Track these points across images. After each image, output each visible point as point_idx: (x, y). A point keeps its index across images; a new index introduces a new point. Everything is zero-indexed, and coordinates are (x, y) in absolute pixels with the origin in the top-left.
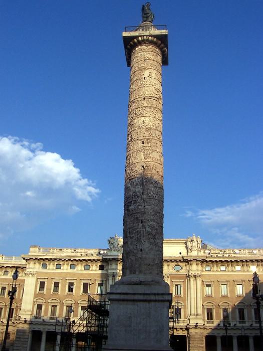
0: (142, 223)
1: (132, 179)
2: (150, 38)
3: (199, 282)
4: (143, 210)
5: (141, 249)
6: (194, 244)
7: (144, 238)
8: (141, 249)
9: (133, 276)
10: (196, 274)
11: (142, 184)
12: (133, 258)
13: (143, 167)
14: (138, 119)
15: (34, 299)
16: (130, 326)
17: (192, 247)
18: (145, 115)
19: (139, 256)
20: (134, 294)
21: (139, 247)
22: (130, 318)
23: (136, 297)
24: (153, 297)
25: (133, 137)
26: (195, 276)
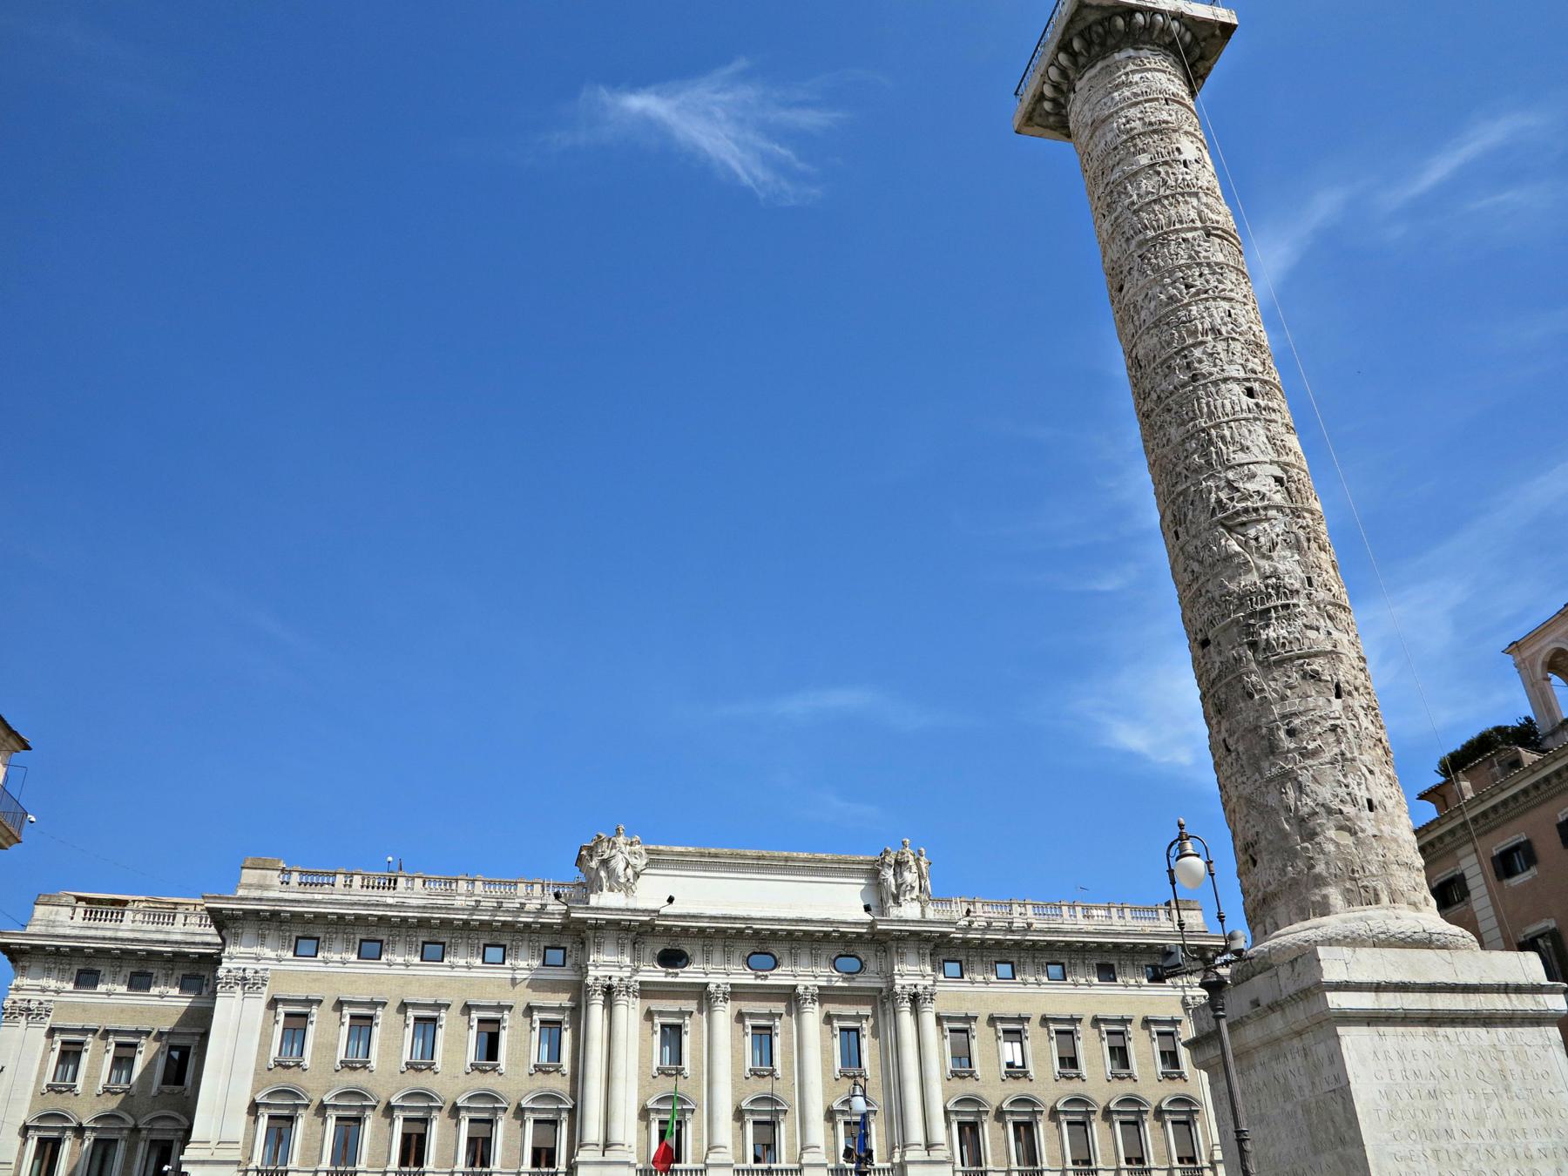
0: (1338, 696)
1: (1243, 524)
2: (1175, 25)
3: (929, 1019)
4: (1329, 648)
5: (1370, 802)
6: (910, 877)
7: (1365, 757)
8: (1370, 802)
9: (1359, 912)
10: (920, 989)
11: (1298, 547)
12: (1346, 839)
13: (1278, 480)
14: (1211, 303)
15: (255, 1091)
16: (1449, 1133)
17: (898, 886)
18: (1228, 294)
19: (1371, 831)
20: (1432, 988)
21: (1362, 795)
22: (1433, 1094)
23: (1442, 1002)
24: (1499, 1003)
25: (1205, 368)
26: (915, 999)
